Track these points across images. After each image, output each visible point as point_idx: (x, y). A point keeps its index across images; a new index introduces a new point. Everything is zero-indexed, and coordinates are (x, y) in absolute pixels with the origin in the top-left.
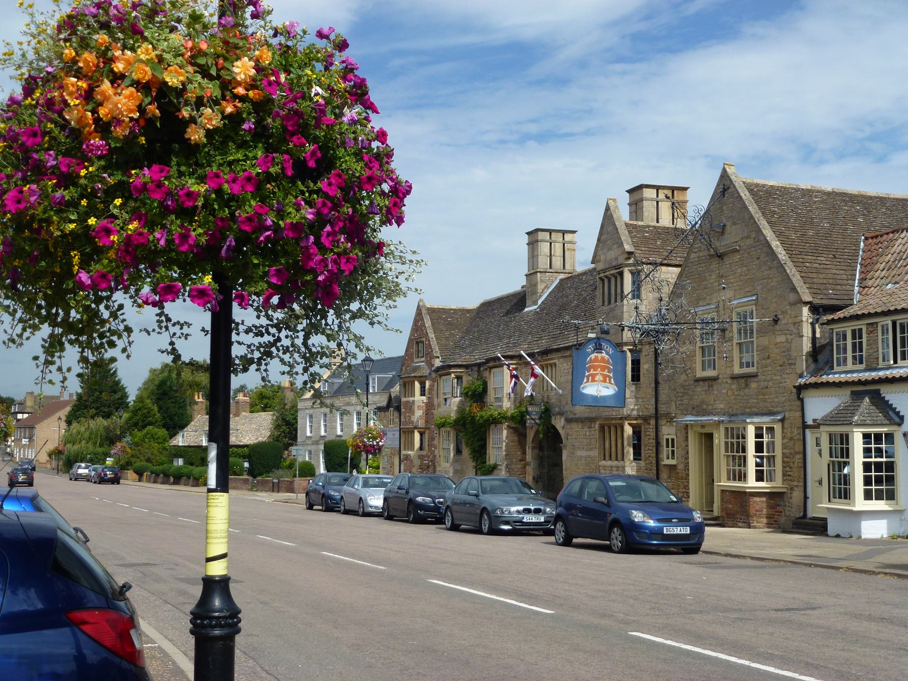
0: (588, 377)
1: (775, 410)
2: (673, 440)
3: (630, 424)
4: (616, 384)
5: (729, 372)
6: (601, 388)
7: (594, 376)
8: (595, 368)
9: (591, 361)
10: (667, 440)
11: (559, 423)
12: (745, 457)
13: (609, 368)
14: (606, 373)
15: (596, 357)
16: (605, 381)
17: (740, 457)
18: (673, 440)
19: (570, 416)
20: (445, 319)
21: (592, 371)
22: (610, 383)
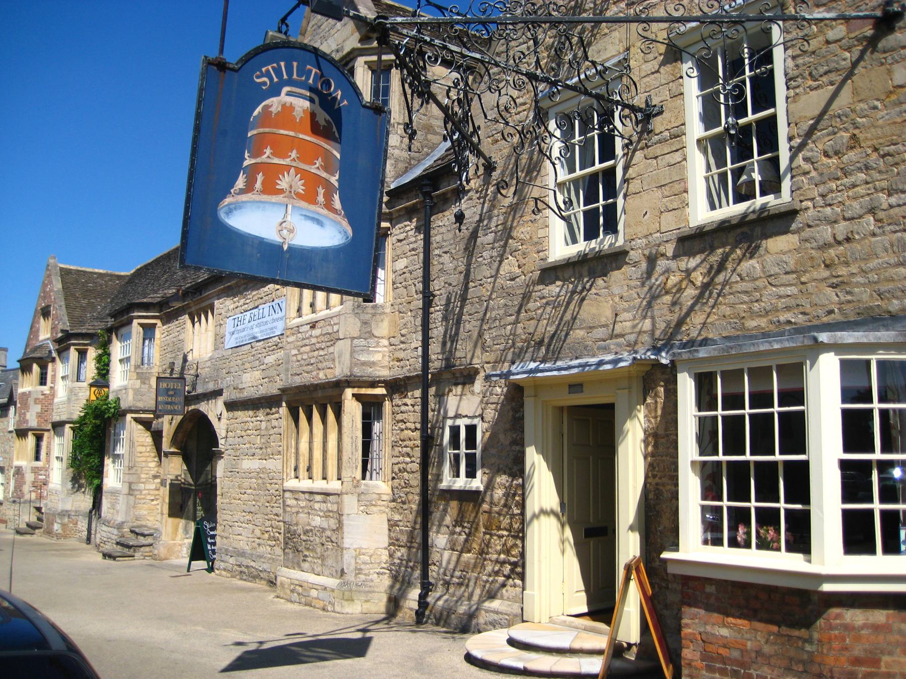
0: (251, 173)
2: (471, 430)
3: (357, 397)
4: (351, 213)
5: (669, 222)
7: (273, 173)
10: (455, 430)
11: (214, 410)
12: (803, 468)
13: (327, 155)
16: (309, 197)
17: (767, 472)
18: (471, 430)
19: (235, 396)
20: (84, 284)
22: (328, 206)
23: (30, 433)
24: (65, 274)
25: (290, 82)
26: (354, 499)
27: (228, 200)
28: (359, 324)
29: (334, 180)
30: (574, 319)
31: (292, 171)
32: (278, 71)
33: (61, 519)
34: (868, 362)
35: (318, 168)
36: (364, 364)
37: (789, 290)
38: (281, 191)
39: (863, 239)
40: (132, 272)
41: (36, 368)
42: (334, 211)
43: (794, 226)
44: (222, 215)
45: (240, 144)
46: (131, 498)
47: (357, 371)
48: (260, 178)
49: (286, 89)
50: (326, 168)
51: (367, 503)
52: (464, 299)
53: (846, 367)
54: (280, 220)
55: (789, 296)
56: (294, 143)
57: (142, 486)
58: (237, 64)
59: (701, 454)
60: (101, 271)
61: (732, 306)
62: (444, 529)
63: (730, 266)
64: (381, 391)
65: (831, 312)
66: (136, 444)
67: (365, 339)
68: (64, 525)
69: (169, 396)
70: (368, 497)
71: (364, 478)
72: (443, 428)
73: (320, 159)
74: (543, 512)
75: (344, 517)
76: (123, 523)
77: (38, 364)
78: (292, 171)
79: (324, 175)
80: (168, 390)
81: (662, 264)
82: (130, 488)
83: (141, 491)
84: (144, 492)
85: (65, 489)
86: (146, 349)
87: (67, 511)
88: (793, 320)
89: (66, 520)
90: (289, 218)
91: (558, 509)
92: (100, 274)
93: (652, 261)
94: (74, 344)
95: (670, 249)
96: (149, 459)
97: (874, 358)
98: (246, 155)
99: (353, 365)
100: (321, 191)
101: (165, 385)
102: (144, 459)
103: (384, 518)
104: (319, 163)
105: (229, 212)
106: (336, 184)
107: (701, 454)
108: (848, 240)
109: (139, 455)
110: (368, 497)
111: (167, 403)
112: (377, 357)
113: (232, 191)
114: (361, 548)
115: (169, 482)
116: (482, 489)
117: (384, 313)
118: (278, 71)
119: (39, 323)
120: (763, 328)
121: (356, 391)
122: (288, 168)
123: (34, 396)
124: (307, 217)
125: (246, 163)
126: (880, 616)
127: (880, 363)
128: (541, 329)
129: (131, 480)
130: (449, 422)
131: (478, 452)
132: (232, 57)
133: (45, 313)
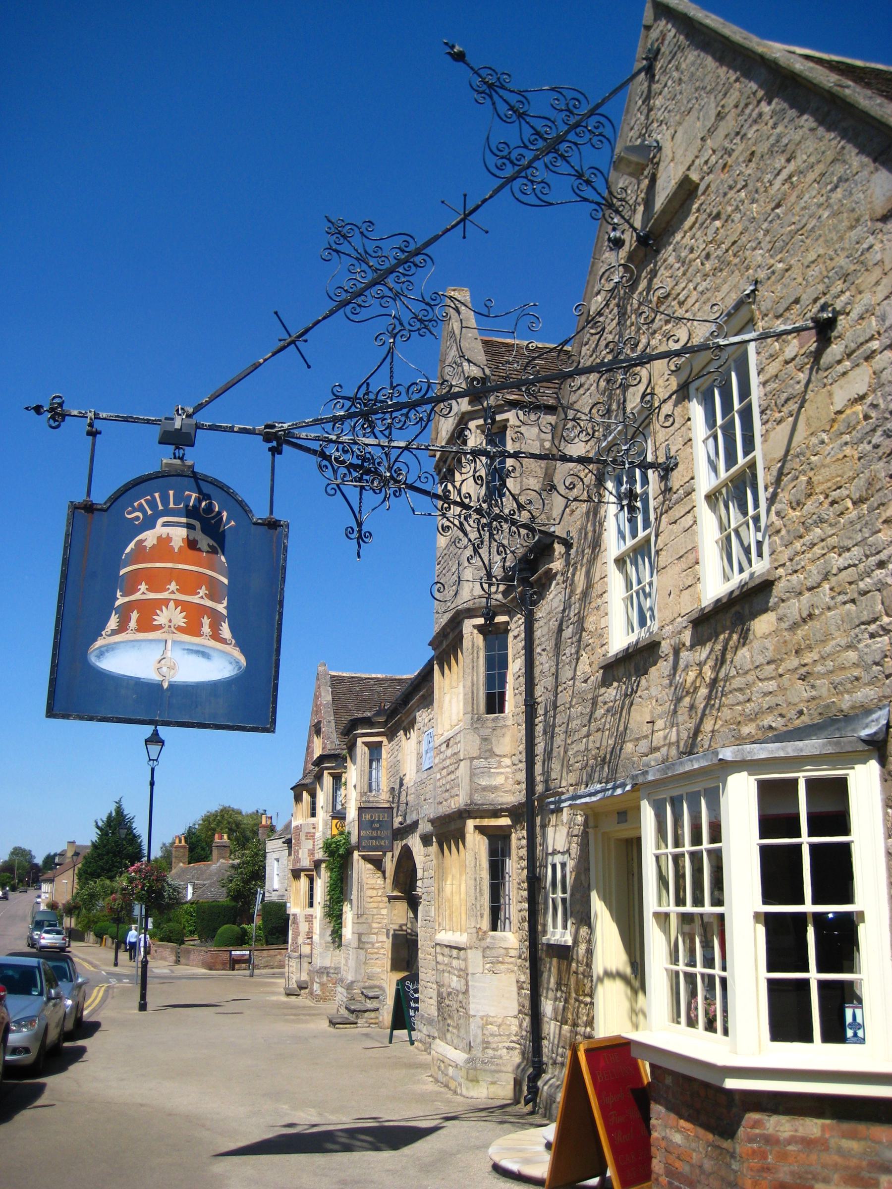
0: (124, 613)
1: (846, 702)
3: (480, 829)
4: (242, 641)
6: (175, 655)
7: (148, 610)
8: (157, 581)
9: (141, 554)
13: (212, 584)
14: (200, 598)
15: (163, 542)
16: (193, 629)
20: (358, 694)
21: (143, 592)
22: (216, 636)
23: (302, 874)
24: (336, 682)
25: (167, 512)
26: (479, 954)
27: (100, 643)
28: (478, 742)
29: (222, 608)
30: (626, 729)
31: (172, 604)
32: (152, 504)
33: (320, 977)
34: (795, 781)
35: (202, 597)
36: (485, 789)
37: (772, 685)
38: (160, 627)
39: (822, 613)
40: (416, 674)
41: (306, 796)
42: (223, 641)
43: (772, 601)
44: (93, 659)
45: (113, 582)
46: (362, 952)
47: (478, 798)
48: (135, 616)
49: (161, 521)
50: (211, 597)
51: (494, 962)
52: (555, 707)
53: (766, 789)
54: (159, 658)
55: (771, 693)
56: (171, 574)
57: (374, 938)
58: (105, 503)
59: (765, 902)
60: (379, 676)
61: (731, 707)
62: (550, 993)
63: (729, 656)
64: (505, 821)
65: (801, 713)
66: (366, 887)
67: (486, 759)
68: (322, 985)
69: (373, 829)
70: (494, 953)
71: (494, 928)
72: (546, 867)
73: (204, 587)
74: (608, 974)
75: (470, 977)
76: (352, 982)
77: (308, 792)
78: (172, 604)
79: (209, 603)
80: (372, 822)
81: (684, 654)
82: (360, 940)
83: (373, 944)
84: (377, 945)
85: (323, 941)
86: (374, 772)
87: (326, 968)
88: (774, 725)
89: (325, 979)
90: (169, 654)
91: (628, 971)
92: (378, 679)
93: (677, 652)
94: (327, 768)
95: (687, 637)
96: (381, 905)
97: (802, 777)
98: (119, 594)
99: (475, 789)
100: (206, 621)
101: (368, 817)
102: (375, 905)
103: (513, 978)
104: (203, 591)
105: (101, 654)
106: (225, 612)
107: (765, 902)
108: (810, 616)
109: (369, 900)
110: (494, 953)
111: (372, 838)
112: (499, 780)
113: (103, 633)
114: (488, 1016)
115: (392, 932)
116: (570, 943)
117: (506, 726)
118: (152, 504)
119: (313, 742)
120: (753, 736)
121: (478, 822)
122: (166, 602)
123: (305, 830)
124: (190, 651)
125: (117, 603)
126: (812, 1127)
127: (811, 783)
128: (604, 743)
129: (361, 931)
130: (550, 858)
131: (567, 896)
132: (100, 497)
133: (318, 732)
